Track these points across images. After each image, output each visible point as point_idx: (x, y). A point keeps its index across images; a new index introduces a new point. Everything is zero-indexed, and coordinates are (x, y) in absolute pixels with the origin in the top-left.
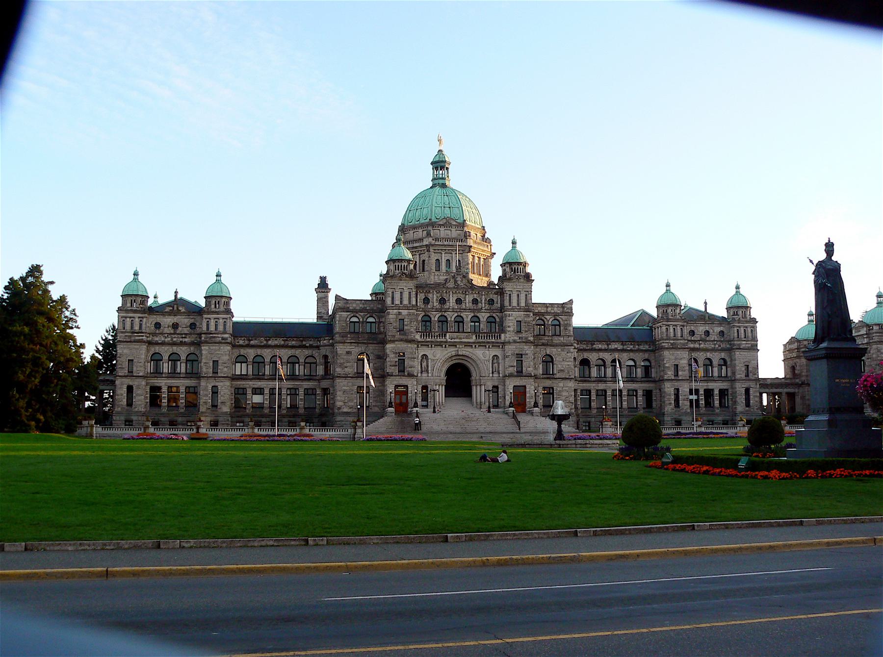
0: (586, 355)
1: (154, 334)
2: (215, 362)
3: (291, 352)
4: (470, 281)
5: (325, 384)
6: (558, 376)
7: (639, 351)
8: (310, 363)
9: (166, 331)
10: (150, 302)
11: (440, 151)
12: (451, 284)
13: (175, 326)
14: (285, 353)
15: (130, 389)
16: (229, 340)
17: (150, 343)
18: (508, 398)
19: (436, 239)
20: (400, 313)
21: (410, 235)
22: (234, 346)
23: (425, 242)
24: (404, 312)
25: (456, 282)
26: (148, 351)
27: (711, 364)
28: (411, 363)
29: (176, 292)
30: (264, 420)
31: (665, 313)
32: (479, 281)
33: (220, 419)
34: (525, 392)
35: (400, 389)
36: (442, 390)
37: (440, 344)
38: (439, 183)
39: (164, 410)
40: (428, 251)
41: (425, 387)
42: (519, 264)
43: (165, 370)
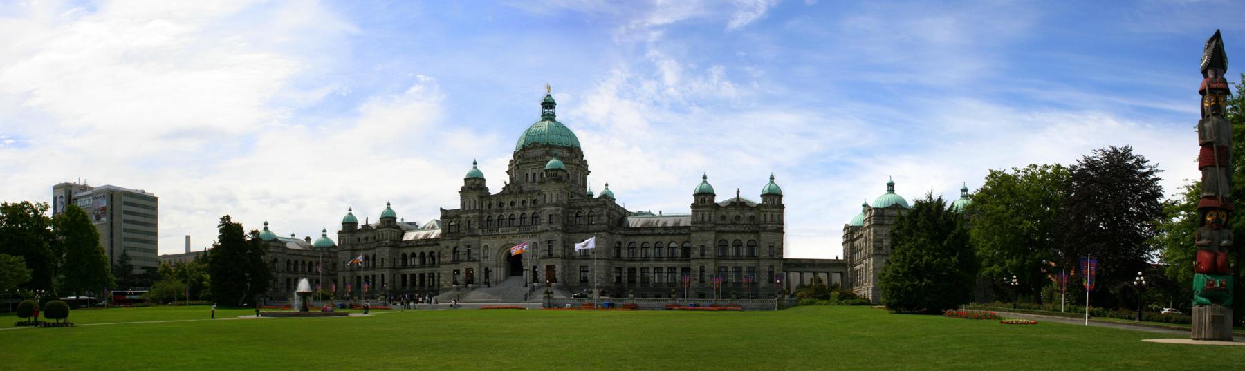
0: (632, 239)
24: (471, 215)
31: (703, 201)
37: (494, 237)
41: (487, 269)
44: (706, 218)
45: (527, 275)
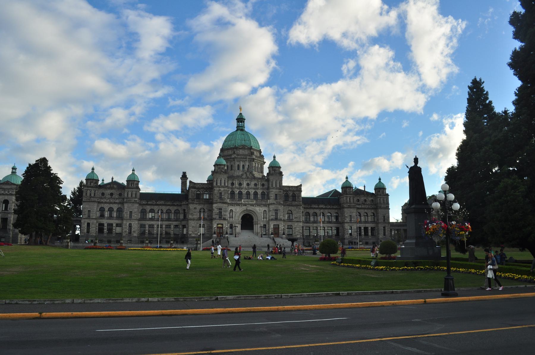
0: (308, 210)
1: (101, 198)
2: (131, 212)
3: (168, 207)
4: (253, 175)
5: (184, 223)
6: (295, 220)
7: (333, 209)
8: (177, 212)
9: (107, 197)
10: (100, 183)
11: (241, 114)
12: (244, 176)
13: (112, 194)
14: (165, 208)
15: (88, 224)
16: (138, 201)
17: (99, 202)
18: (270, 230)
19: (238, 155)
20: (220, 190)
21: (226, 153)
22: (140, 204)
23: (233, 156)
24: (222, 189)
25: (246, 175)
26: (98, 206)
27: (367, 216)
29: (113, 178)
30: (154, 240)
32: (257, 175)
33: (133, 239)
34: (279, 228)
35: (219, 226)
36: (239, 226)
38: (240, 128)
39: (105, 235)
40: (234, 160)
42: (277, 167)
43: (106, 216)
44: (352, 201)
45: (257, 228)
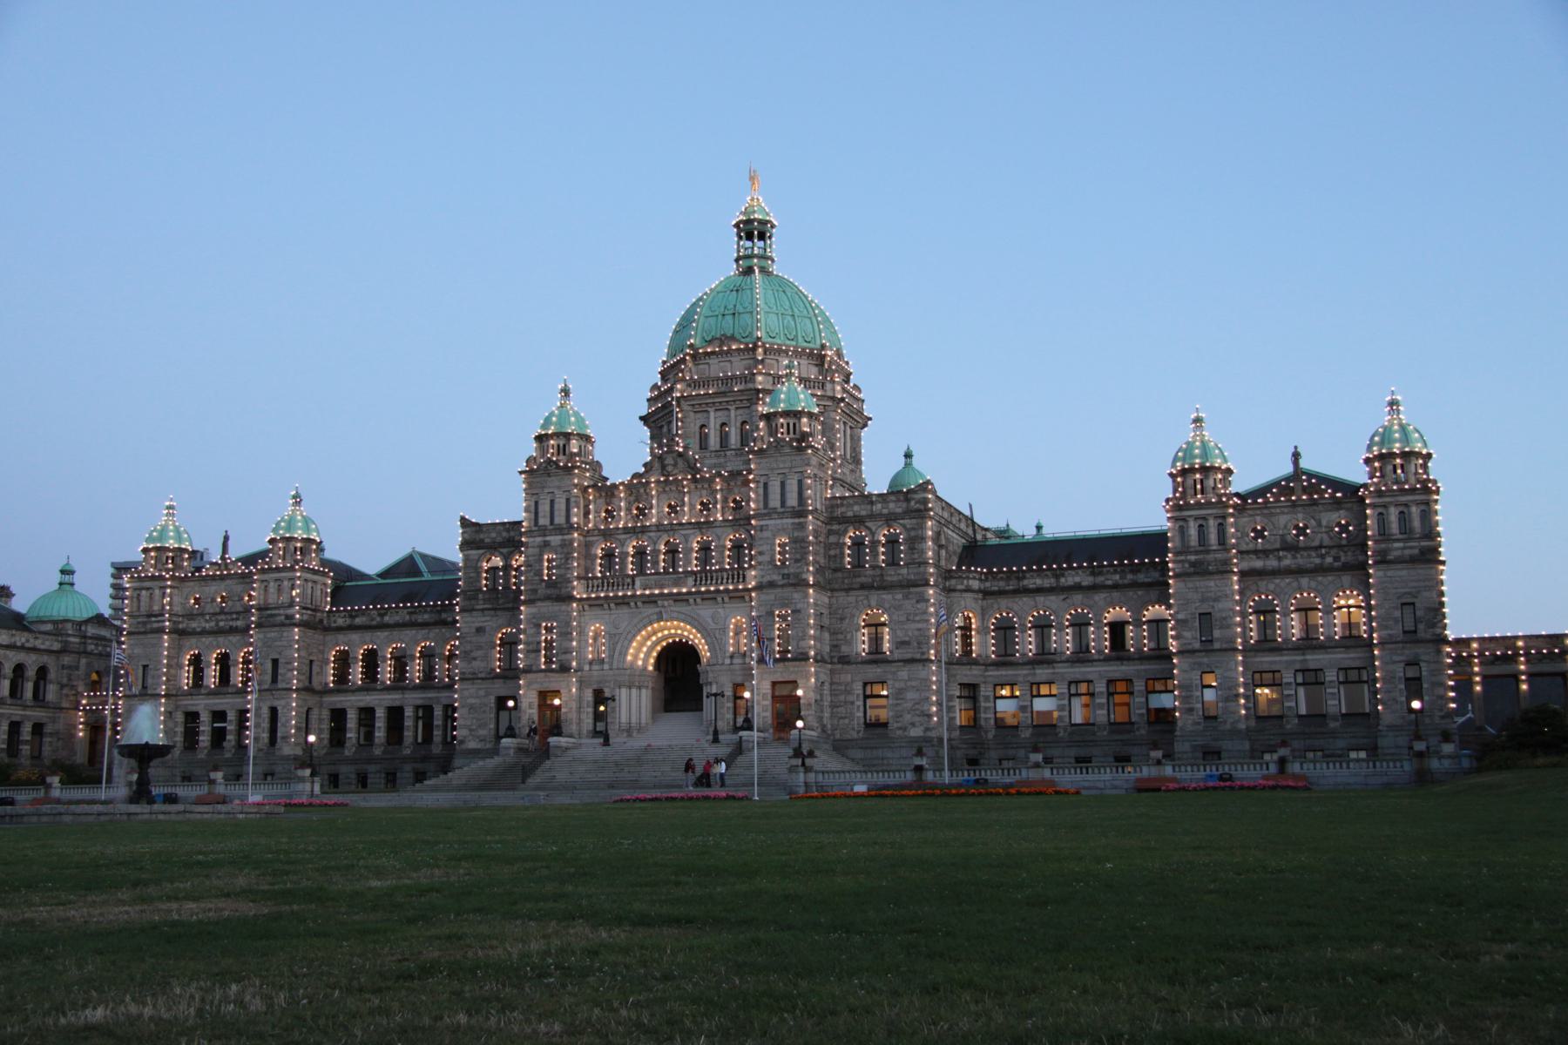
2: (275, 662)
6: (896, 656)
7: (1134, 585)
20: (546, 544)
24: (555, 540)
28: (565, 644)
29: (226, 538)
30: (372, 768)
37: (623, 602)
39: (202, 755)
44: (1213, 538)
